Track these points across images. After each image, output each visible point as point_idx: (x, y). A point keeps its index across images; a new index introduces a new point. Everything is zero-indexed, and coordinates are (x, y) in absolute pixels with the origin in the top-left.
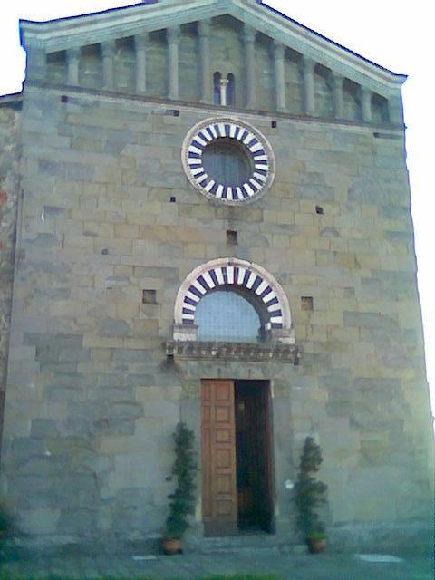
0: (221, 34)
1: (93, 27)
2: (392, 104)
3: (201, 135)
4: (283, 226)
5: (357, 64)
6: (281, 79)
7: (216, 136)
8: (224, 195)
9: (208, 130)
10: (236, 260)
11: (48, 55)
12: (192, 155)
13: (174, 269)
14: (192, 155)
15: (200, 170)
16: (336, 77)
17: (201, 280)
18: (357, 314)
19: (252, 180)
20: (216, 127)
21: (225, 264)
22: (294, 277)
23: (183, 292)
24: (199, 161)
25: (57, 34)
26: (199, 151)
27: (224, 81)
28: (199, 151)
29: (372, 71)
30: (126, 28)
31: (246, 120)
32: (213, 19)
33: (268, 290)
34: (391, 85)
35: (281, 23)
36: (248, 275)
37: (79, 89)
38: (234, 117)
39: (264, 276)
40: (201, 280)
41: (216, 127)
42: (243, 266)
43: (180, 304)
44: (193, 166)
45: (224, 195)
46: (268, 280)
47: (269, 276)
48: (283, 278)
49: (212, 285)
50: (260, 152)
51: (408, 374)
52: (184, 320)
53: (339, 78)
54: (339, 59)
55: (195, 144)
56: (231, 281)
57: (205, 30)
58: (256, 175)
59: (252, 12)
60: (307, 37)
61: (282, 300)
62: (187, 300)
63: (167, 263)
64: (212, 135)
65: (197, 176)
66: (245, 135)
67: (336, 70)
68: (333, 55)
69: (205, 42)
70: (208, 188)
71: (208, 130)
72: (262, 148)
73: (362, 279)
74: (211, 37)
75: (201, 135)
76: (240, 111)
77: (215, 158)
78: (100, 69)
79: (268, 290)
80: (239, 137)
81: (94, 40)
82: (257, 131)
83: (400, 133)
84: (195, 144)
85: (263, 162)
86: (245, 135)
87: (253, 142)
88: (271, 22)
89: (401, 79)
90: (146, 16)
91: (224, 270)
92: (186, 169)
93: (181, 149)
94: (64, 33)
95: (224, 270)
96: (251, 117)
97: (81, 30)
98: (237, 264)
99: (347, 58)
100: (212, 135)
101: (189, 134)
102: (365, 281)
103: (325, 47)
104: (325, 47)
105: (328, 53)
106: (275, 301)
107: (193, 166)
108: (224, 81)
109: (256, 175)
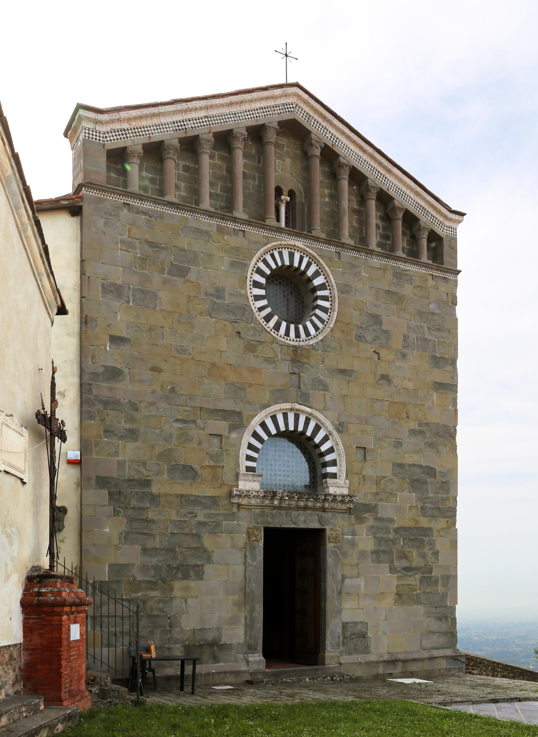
0: (284, 141)
1: (155, 121)
2: (446, 244)
3: (265, 262)
4: (343, 372)
5: (417, 194)
6: (345, 204)
7: (280, 264)
8: (287, 333)
9: (272, 256)
10: (298, 406)
11: (107, 150)
12: (256, 284)
13: (239, 414)
14: (256, 284)
15: (264, 302)
16: (399, 208)
17: (263, 425)
18: (401, 466)
19: (314, 318)
20: (281, 254)
21: (287, 409)
22: (350, 426)
23: (248, 438)
24: (262, 292)
25: (117, 126)
26: (263, 281)
27: (285, 198)
28: (263, 281)
29: (432, 205)
30: (190, 124)
31: (312, 248)
32: (280, 123)
33: (326, 439)
34: (447, 223)
35: (348, 137)
36: (307, 421)
37: (141, 198)
38: (299, 243)
39: (323, 424)
40: (263, 425)
41: (281, 254)
42: (303, 412)
43: (244, 451)
44: (257, 298)
45: (287, 333)
46: (326, 428)
47: (328, 424)
48: (340, 428)
49: (274, 431)
50: (323, 287)
51: (442, 523)
52: (246, 467)
53: (401, 209)
54: (400, 186)
55: (259, 272)
56: (291, 428)
57: (271, 137)
58: (318, 311)
59: (320, 120)
60: (373, 157)
61: (338, 450)
62: (251, 447)
63: (229, 405)
64: (276, 263)
65: (261, 309)
66: (308, 265)
67: (399, 200)
68: (396, 182)
69: (271, 150)
70: (272, 323)
71: (272, 256)
72: (325, 281)
73: (410, 431)
74: (277, 145)
75: (265, 262)
76: (306, 237)
77: (278, 290)
78: (161, 171)
79: (326, 439)
80: (303, 268)
81: (156, 137)
82: (321, 261)
83: (450, 277)
84: (259, 272)
85: (325, 298)
86: (308, 265)
87: (317, 274)
88: (338, 135)
89: (457, 217)
90: (211, 113)
91: (285, 416)
92: (251, 299)
93: (247, 278)
94: (126, 126)
95: (285, 416)
96: (316, 245)
97: (144, 123)
98: (298, 410)
99: (408, 187)
100: (276, 263)
101: (254, 260)
102: (413, 432)
103: (389, 171)
104: (389, 171)
105: (392, 179)
106: (331, 450)
107: (257, 298)
108: (285, 198)
109: (318, 311)
